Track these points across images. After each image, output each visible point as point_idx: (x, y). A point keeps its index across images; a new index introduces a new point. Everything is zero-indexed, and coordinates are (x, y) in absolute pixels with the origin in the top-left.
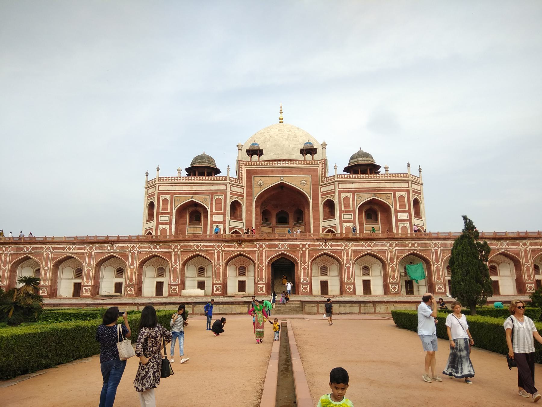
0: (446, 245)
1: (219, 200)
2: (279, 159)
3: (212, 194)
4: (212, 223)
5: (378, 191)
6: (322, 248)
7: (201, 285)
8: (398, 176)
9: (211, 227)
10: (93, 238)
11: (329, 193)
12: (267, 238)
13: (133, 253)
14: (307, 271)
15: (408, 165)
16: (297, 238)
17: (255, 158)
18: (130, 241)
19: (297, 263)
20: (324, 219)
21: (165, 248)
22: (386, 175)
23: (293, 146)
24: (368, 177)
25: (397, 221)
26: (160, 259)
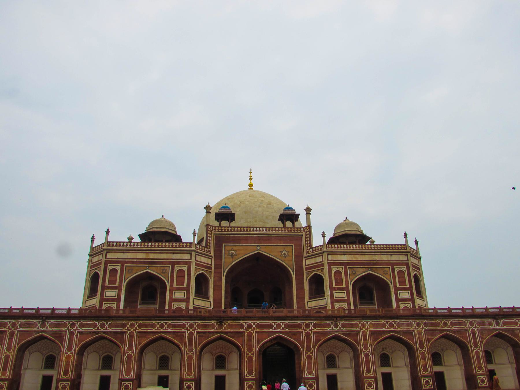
0: (483, 324)
1: (181, 271)
3: (173, 264)
4: (172, 300)
6: (331, 328)
8: (395, 248)
9: (170, 306)
10: (18, 311)
12: (257, 315)
13: (72, 334)
14: (313, 361)
15: (406, 235)
16: (299, 315)
17: (225, 223)
18: (68, 315)
19: (298, 349)
20: (310, 298)
21: (117, 326)
23: (267, 213)
24: (362, 247)
25: (398, 301)
26: (107, 341)
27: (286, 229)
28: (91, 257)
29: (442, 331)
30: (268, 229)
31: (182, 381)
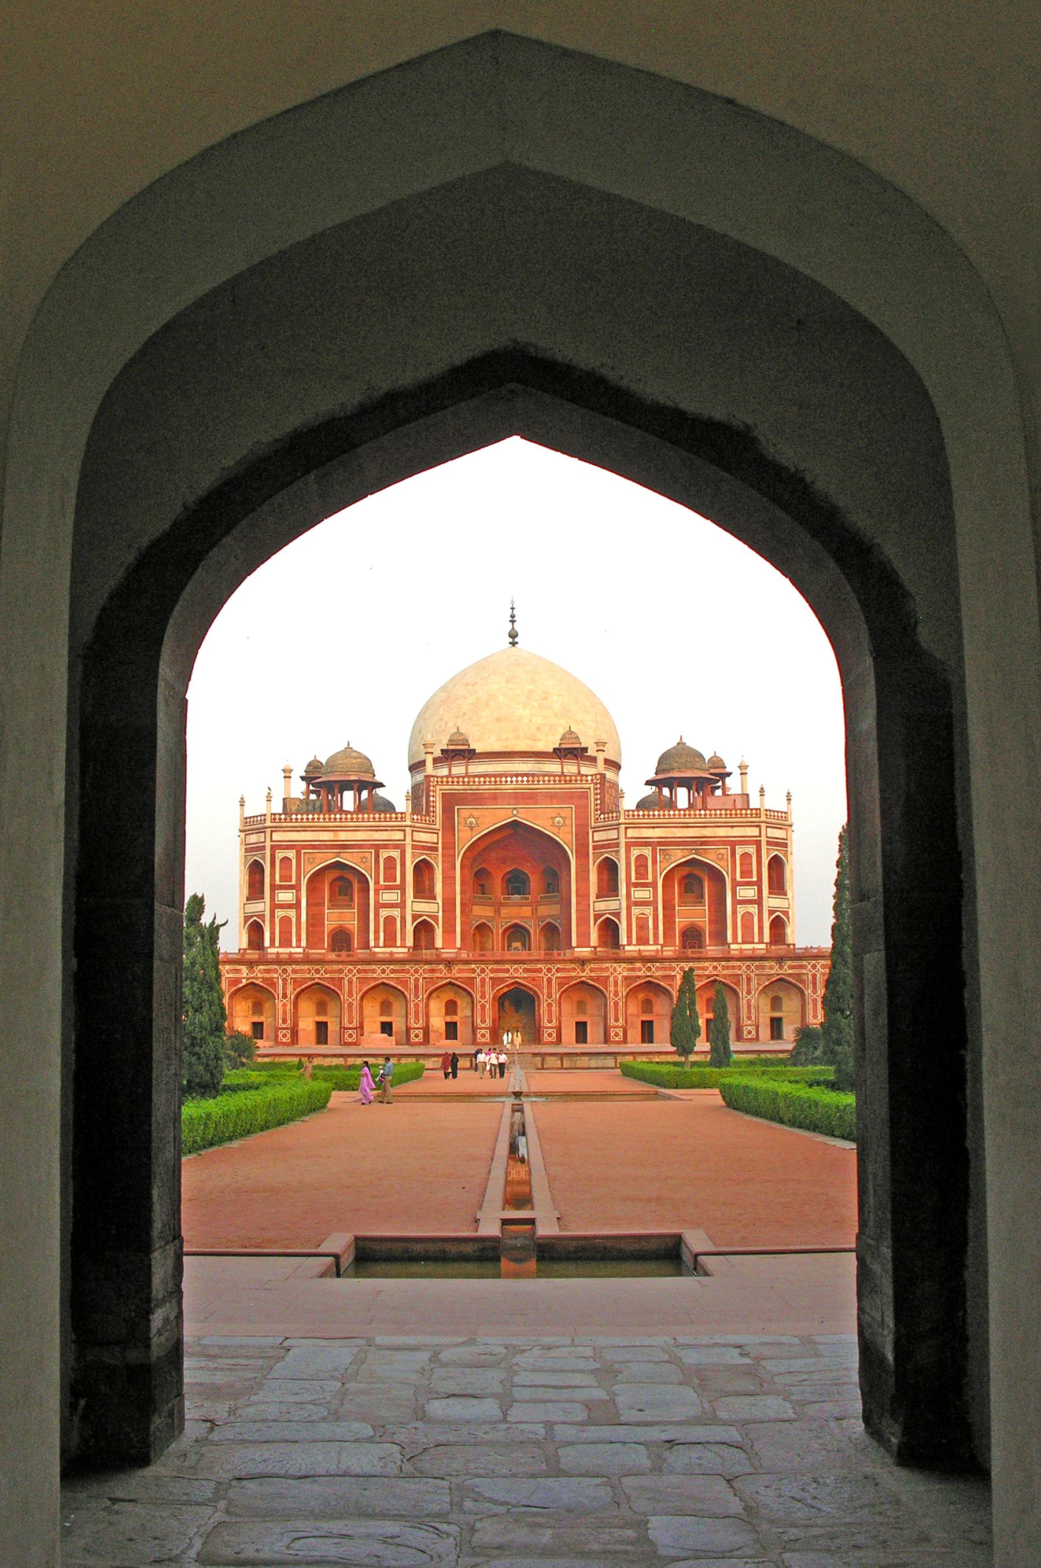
0: (763, 967)
1: (390, 860)
2: (508, 750)
3: (377, 848)
4: (379, 906)
5: (703, 843)
7: (387, 1028)
11: (609, 846)
13: (284, 980)
14: (553, 1009)
15: (762, 790)
19: (538, 997)
21: (334, 972)
22: (718, 812)
23: (539, 720)
24: (685, 815)
25: (736, 902)
27: (563, 778)
28: (243, 834)
29: (708, 976)
30: (531, 779)
31: (408, 1030)
